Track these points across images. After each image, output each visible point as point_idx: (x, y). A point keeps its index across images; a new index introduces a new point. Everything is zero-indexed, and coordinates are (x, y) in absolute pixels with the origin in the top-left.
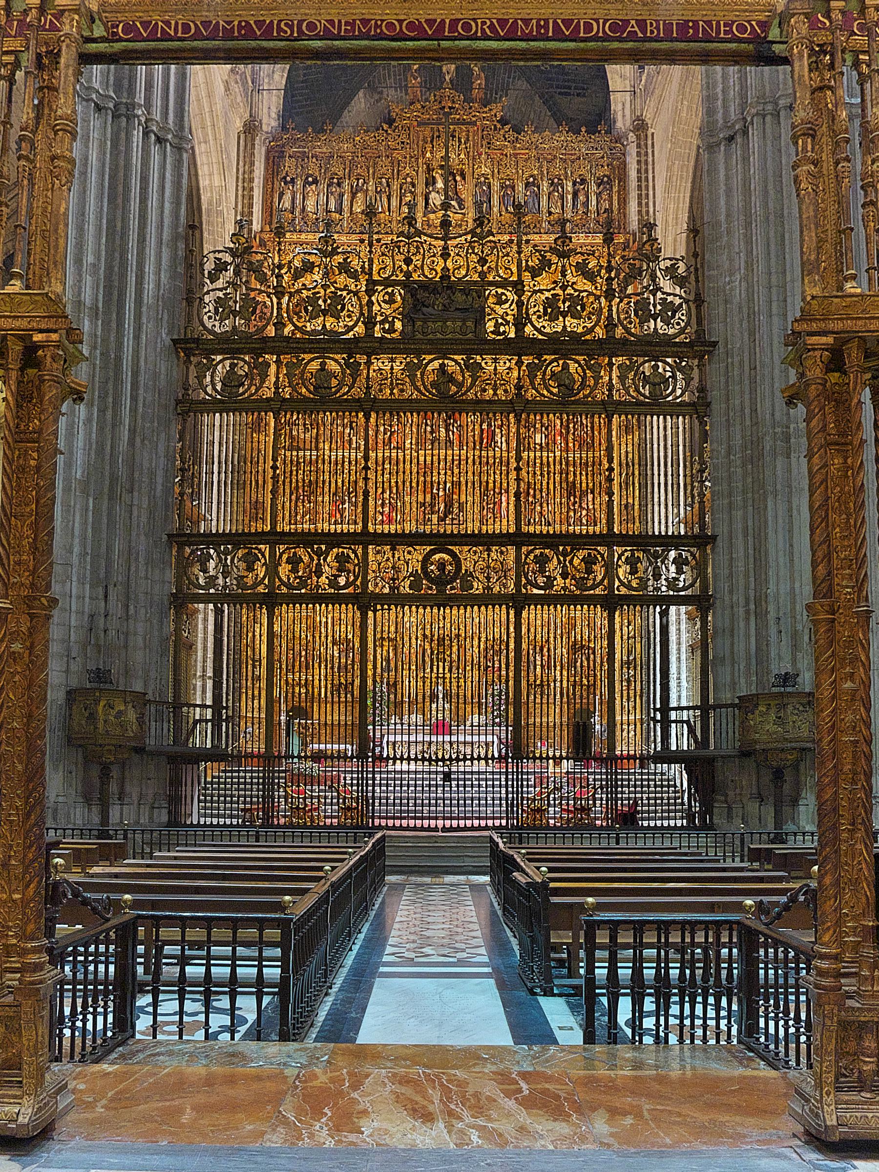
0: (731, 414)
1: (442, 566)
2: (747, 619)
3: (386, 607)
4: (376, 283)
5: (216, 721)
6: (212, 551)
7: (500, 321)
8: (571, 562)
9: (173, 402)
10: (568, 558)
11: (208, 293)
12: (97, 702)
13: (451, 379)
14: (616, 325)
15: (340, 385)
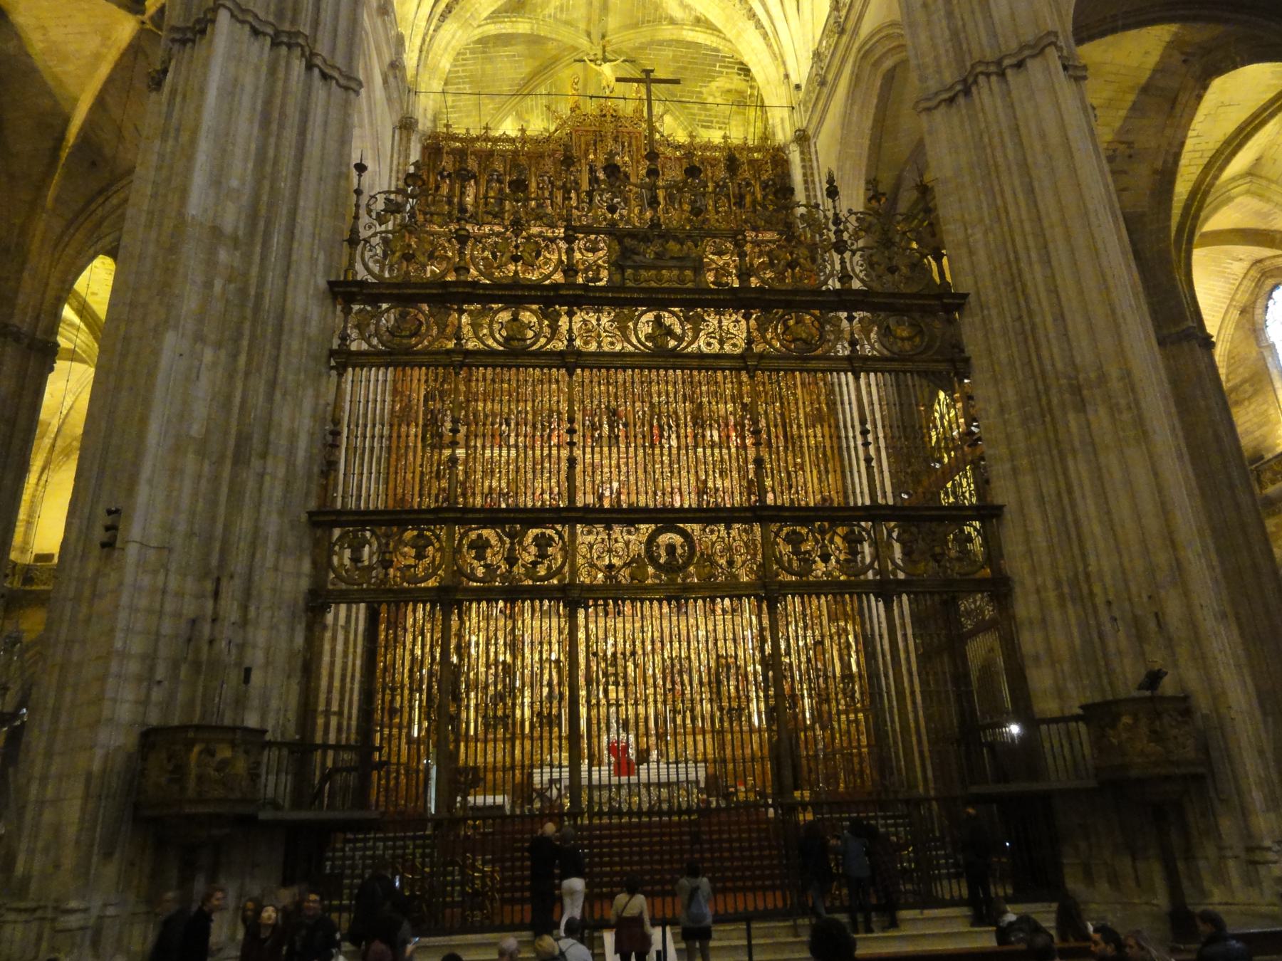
1: (671, 549)
2: (1062, 606)
4: (575, 229)
8: (831, 541)
9: (326, 352)
10: (827, 537)
13: (669, 332)
14: (851, 278)
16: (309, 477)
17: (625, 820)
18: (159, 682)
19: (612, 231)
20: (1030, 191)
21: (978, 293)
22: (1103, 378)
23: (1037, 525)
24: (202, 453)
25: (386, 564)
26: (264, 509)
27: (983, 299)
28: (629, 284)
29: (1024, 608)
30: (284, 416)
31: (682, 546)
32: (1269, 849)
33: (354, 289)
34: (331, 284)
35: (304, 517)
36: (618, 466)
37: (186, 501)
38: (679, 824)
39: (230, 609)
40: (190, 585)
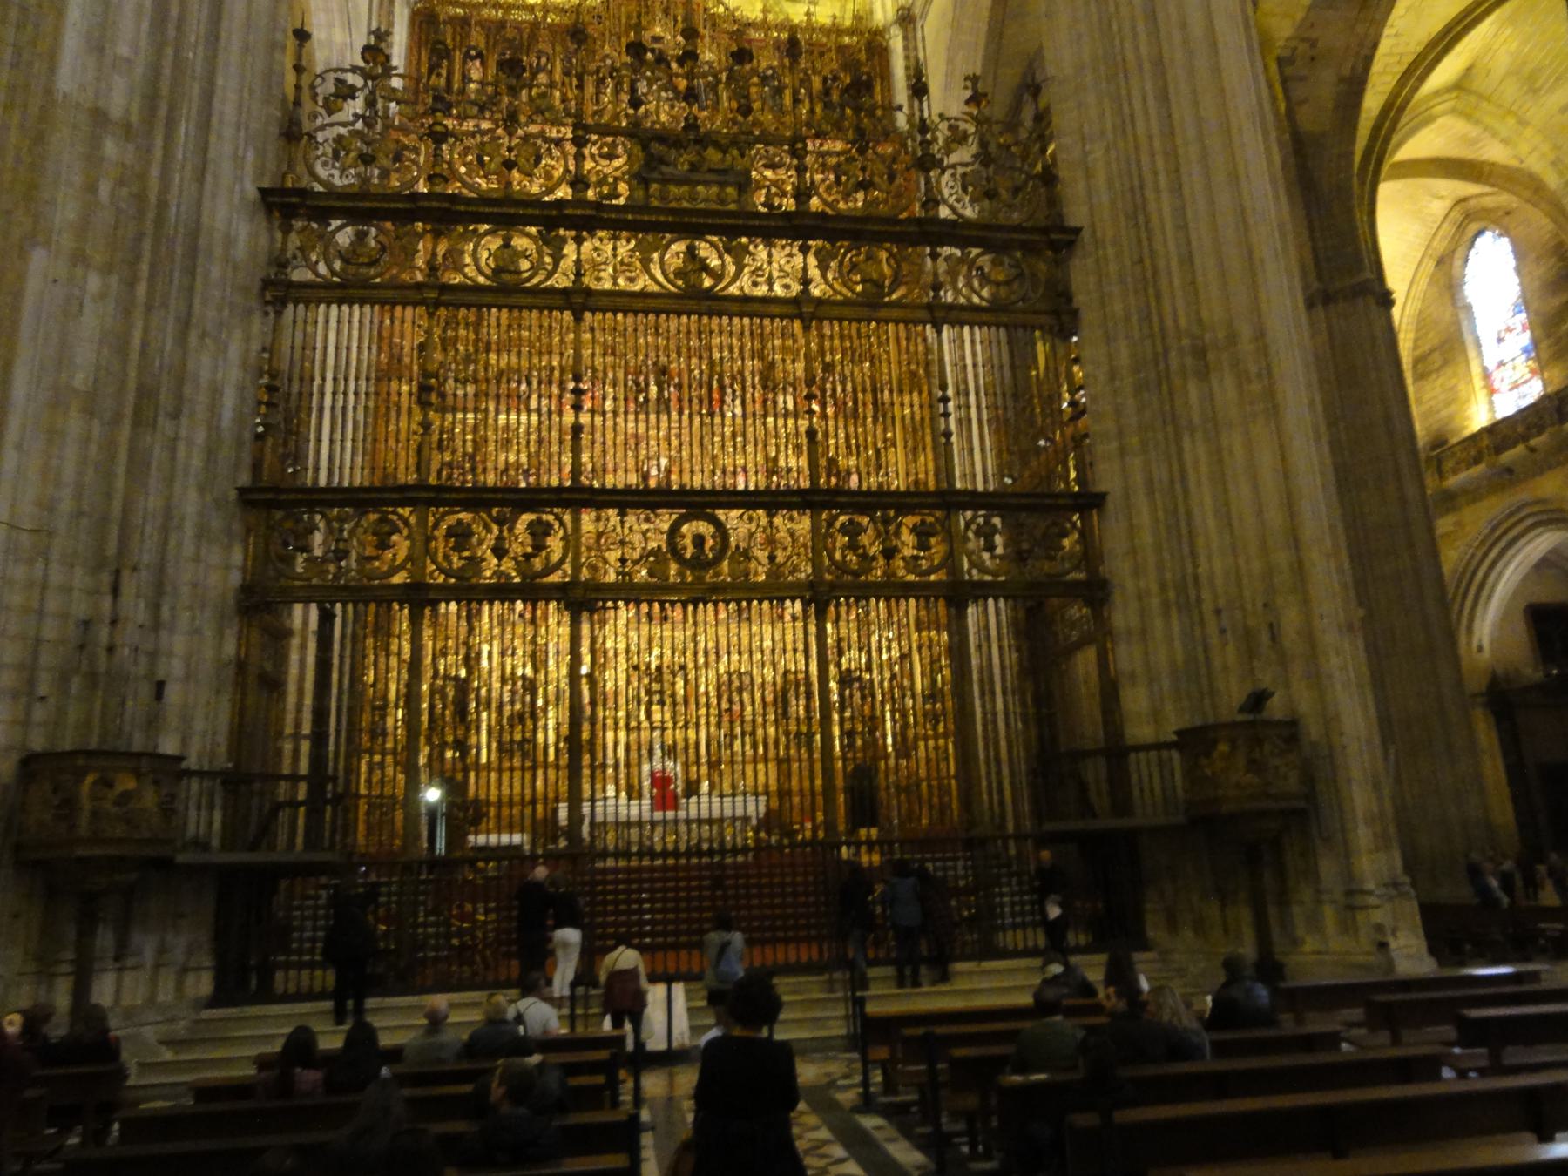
0: (1110, 324)
1: (699, 540)
2: (1166, 614)
3: (610, 604)
4: (588, 129)
5: (315, 804)
6: (318, 517)
7: (773, 190)
9: (257, 284)
11: (323, 127)
12: (80, 774)
13: (704, 267)
15: (534, 270)
16: (239, 443)
17: (659, 862)
18: (43, 698)
19: (636, 132)
20: (1164, 96)
21: (1093, 225)
22: (1232, 338)
23: (1144, 518)
24: (89, 411)
25: (342, 554)
26: (177, 486)
27: (1099, 234)
28: (655, 203)
29: (1122, 616)
30: (203, 364)
31: (713, 537)
32: (1370, 893)
33: (294, 200)
34: (264, 192)
35: (233, 495)
36: (668, 439)
37: (69, 470)
38: (699, 867)
39: (135, 609)
40: (80, 578)
